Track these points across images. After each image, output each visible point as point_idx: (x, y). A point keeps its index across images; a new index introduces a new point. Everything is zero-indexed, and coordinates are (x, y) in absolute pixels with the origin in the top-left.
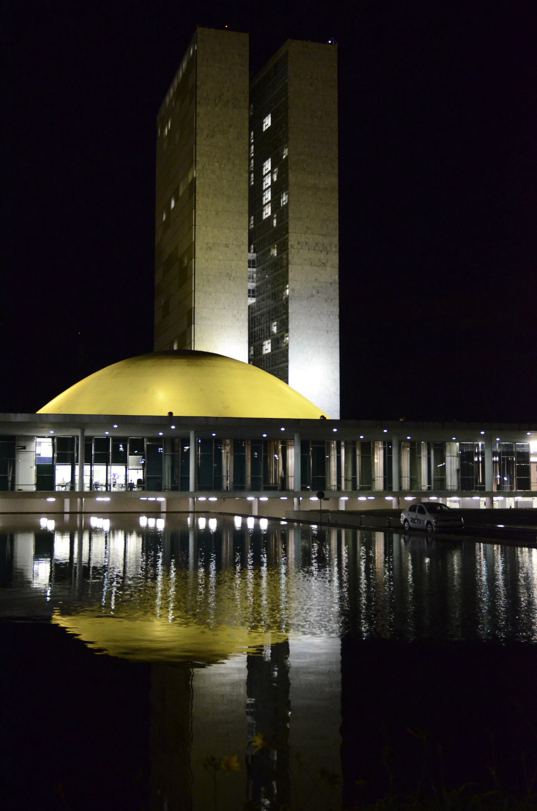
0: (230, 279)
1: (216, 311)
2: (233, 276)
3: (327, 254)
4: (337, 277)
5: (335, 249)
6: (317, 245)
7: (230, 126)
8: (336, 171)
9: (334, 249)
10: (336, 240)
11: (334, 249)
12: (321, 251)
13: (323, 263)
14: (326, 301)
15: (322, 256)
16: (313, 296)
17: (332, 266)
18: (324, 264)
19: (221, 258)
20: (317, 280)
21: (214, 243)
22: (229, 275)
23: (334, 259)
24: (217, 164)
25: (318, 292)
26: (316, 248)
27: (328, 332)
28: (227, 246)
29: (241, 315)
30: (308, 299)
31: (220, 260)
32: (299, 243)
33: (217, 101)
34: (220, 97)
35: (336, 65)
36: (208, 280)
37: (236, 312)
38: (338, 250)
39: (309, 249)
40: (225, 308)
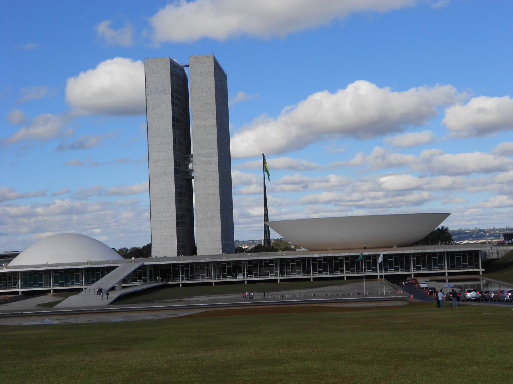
4: (217, 168)
5: (216, 155)
7: (162, 103)
8: (215, 117)
10: (216, 150)
14: (212, 180)
15: (210, 159)
16: (206, 179)
17: (215, 163)
22: (165, 173)
23: (216, 159)
24: (157, 122)
25: (208, 176)
28: (163, 160)
35: (213, 64)
37: (169, 190)
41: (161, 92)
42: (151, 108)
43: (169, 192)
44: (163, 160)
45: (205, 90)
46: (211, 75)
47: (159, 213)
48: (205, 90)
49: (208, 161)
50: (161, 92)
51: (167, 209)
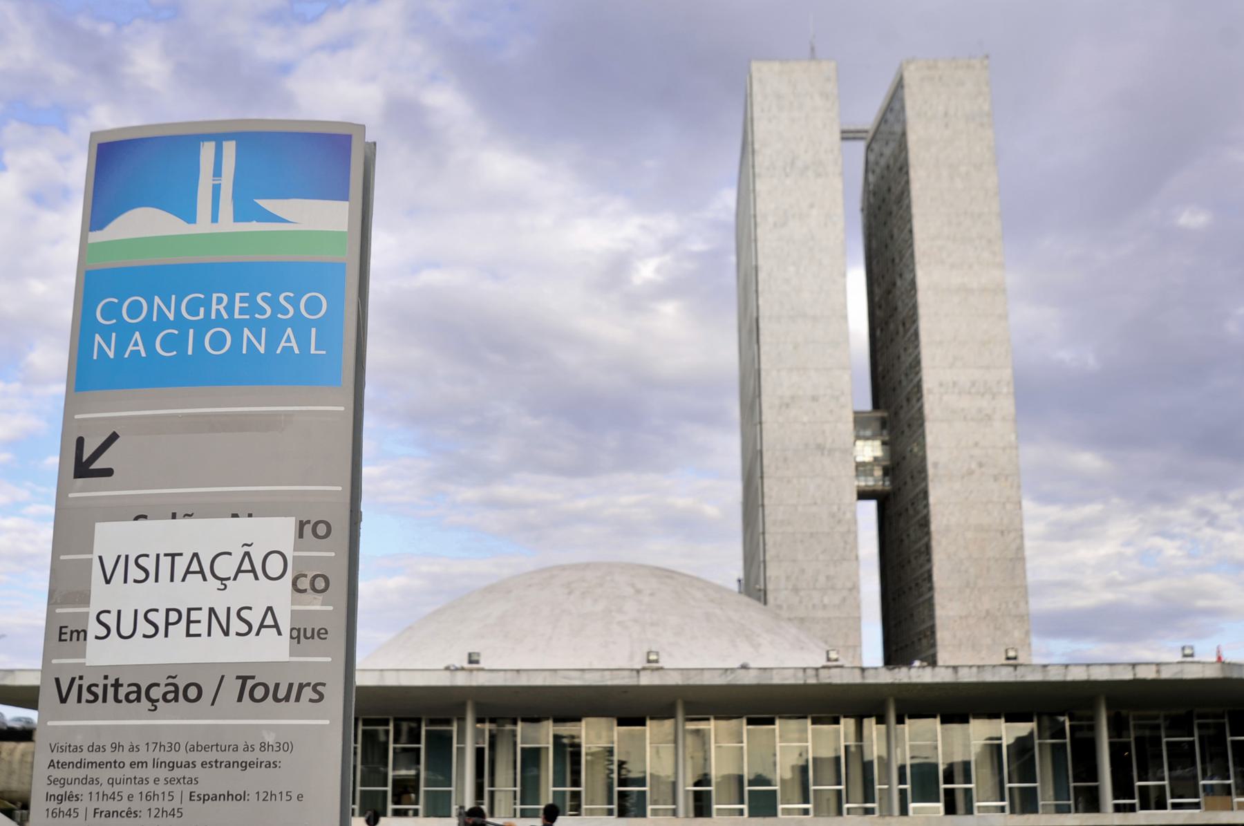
0: (823, 454)
1: (800, 509)
2: (828, 446)
3: (993, 398)
6: (973, 384)
7: (812, 206)
9: (1005, 390)
11: (1005, 390)
12: (983, 395)
13: (987, 415)
14: (996, 478)
17: (1003, 419)
18: (989, 417)
19: (805, 419)
20: (976, 444)
21: (793, 398)
24: (792, 269)
25: (981, 465)
26: (973, 390)
27: (1002, 533)
28: (815, 399)
29: (844, 513)
30: (963, 477)
31: (804, 424)
32: (941, 385)
33: (788, 170)
34: (793, 163)
36: (785, 460)
37: (835, 508)
38: (1012, 390)
39: (960, 393)
40: (815, 504)
41: (806, 168)
42: (771, 220)
43: (833, 516)
44: (815, 399)
45: (963, 169)
46: (982, 125)
47: (796, 590)
48: (963, 169)
49: (980, 410)
50: (806, 168)
51: (828, 578)
